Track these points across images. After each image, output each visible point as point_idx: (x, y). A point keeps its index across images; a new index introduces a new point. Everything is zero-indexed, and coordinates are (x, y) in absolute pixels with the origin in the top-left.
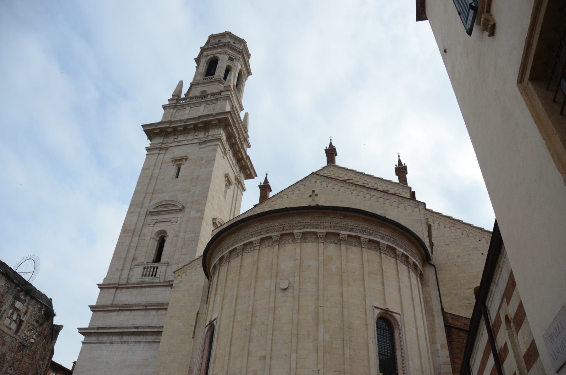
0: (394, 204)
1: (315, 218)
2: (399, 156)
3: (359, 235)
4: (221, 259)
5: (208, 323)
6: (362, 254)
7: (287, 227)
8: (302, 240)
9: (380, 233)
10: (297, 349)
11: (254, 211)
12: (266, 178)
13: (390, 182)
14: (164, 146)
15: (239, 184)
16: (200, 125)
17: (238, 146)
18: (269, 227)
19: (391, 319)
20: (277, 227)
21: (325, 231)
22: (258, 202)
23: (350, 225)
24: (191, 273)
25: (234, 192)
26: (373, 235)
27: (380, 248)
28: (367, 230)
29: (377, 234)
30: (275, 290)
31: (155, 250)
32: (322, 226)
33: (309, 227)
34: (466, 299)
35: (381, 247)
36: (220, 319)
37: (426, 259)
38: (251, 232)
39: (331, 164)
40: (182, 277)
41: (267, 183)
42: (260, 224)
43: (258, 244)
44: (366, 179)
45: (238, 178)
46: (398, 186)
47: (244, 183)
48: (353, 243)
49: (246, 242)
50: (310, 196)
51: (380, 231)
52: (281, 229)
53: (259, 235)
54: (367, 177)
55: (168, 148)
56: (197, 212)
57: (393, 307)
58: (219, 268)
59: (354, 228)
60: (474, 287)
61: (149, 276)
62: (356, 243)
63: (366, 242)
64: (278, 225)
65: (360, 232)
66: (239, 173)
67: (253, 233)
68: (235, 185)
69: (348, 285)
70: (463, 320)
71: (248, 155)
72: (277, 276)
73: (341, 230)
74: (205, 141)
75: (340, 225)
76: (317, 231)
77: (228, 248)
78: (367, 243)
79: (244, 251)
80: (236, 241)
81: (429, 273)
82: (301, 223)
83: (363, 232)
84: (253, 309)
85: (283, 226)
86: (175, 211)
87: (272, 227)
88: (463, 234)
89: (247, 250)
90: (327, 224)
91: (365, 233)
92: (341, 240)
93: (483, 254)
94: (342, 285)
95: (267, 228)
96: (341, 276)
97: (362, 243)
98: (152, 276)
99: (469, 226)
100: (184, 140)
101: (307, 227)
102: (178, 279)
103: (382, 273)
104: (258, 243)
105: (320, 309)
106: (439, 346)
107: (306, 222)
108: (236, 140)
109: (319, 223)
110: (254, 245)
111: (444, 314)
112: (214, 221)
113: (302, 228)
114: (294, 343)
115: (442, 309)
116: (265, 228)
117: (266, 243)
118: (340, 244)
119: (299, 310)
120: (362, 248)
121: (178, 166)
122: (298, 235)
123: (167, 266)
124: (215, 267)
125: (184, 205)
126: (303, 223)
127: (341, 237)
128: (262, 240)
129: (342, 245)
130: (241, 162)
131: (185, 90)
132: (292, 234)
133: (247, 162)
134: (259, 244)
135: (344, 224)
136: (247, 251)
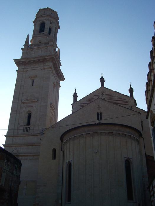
3: (119, 132)
5: (67, 161)
14: (25, 70)
16: (41, 60)
21: (108, 132)
37: (140, 135)
49: (81, 134)
50: (98, 108)
61: (26, 131)
74: (44, 68)
81: (141, 140)
98: (28, 131)
100: (34, 67)
115: (145, 154)
131: (31, 39)
132: (97, 133)
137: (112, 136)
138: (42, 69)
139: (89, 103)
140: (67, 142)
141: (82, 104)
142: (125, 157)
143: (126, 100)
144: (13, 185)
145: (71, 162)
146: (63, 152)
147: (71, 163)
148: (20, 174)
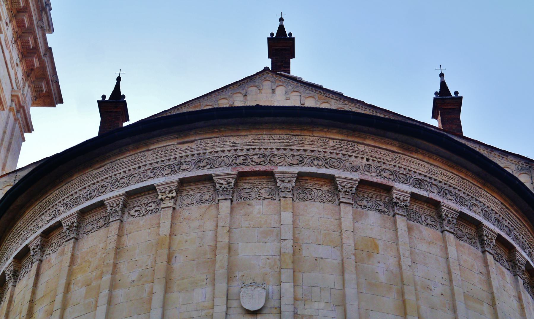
2: (442, 75)
3: (436, 197)
4: (47, 234)
6: (446, 247)
7: (256, 157)
8: (295, 195)
9: (480, 202)
12: (117, 87)
15: (18, 111)
17: (30, 17)
18: (204, 153)
20: (227, 153)
21: (356, 176)
23: (415, 172)
25: (6, 127)
26: (467, 205)
27: (483, 240)
28: (453, 191)
29: (475, 205)
30: (226, 314)
32: (347, 165)
38: (149, 162)
39: (282, 73)
41: (120, 99)
42: (178, 144)
43: (170, 195)
47: (31, 111)
48: (423, 218)
51: (482, 200)
53: (174, 172)
58: (38, 257)
59: (426, 181)
62: (429, 217)
63: (452, 218)
64: (229, 151)
65: (439, 192)
66: (21, 85)
67: (156, 165)
68: (9, 112)
72: (229, 279)
73: (394, 180)
75: (393, 169)
76: (336, 175)
77: (76, 202)
78: (455, 221)
79: (126, 210)
80: (102, 186)
82: (292, 150)
83: (445, 193)
85: (245, 152)
87: (214, 155)
90: (361, 160)
91: (448, 196)
92: (396, 203)
95: (199, 154)
96: (402, 294)
97: (444, 220)
101: (309, 160)
103: (493, 299)
104: (170, 192)
109: (340, 156)
110: (160, 197)
113: (296, 162)
116: (193, 155)
118: (392, 214)
120: (442, 232)
124: (25, 253)
126: (298, 150)
127: (395, 196)
128: (183, 182)
129: (397, 216)
130: (30, 59)
133: (44, 61)
134: (174, 195)
135: (400, 167)
136: (136, 211)
137: (380, 211)
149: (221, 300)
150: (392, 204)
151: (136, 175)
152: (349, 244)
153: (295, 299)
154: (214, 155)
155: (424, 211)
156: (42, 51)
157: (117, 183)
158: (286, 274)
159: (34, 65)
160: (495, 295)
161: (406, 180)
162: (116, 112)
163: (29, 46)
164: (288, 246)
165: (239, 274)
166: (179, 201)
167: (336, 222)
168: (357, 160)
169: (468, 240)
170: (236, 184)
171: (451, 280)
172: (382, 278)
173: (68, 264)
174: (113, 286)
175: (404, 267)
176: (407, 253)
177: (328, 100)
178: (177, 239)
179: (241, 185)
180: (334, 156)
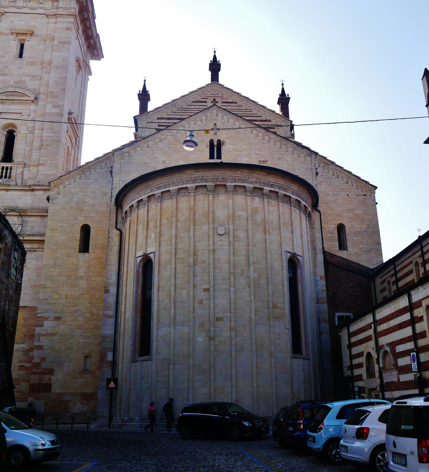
0: (290, 150)
1: (245, 173)
5: (140, 253)
6: (279, 207)
7: (220, 179)
10: (234, 284)
11: (156, 137)
13: (273, 112)
19: (296, 261)
21: (252, 186)
22: (138, 113)
24: (69, 184)
28: (283, 187)
31: (3, 147)
33: (240, 181)
34: (330, 233)
35: (292, 201)
36: (159, 253)
37: (315, 205)
39: (216, 82)
40: (59, 188)
43: (193, 191)
44: (251, 105)
45: (86, 61)
46: (280, 117)
51: (292, 187)
52: (215, 180)
54: (252, 103)
55: (3, 13)
56: (54, 107)
57: (298, 252)
58: (147, 204)
60: (338, 224)
62: (274, 197)
69: (270, 234)
70: (337, 258)
71: (98, 33)
72: (214, 223)
74: (55, 15)
75: (264, 182)
81: (315, 216)
83: (280, 188)
84: (194, 249)
85: (217, 177)
86: (26, 102)
88: (333, 175)
89: (182, 194)
91: (281, 189)
92: (264, 194)
93: (348, 195)
94: (265, 233)
96: (265, 226)
99: (340, 168)
100: (25, 7)
102: (55, 191)
103: (292, 223)
105: (251, 253)
106: (318, 278)
107: (236, 176)
108: (88, 15)
109: (247, 178)
110: (189, 191)
111: (324, 252)
112: (70, 117)
114: (232, 280)
115: (323, 248)
116: (200, 177)
117: (201, 191)
118: (263, 198)
119: (234, 253)
121: (20, 42)
122: (230, 188)
123: (23, 167)
125: (37, 96)
127: (264, 192)
129: (265, 199)
132: (225, 186)
134: (194, 191)
136: (181, 195)
138: (47, 16)
139: (183, 119)
140: (138, 207)
141: (162, 118)
142: (289, 251)
143: (270, 121)
144: (7, 308)
145: (152, 256)
146: (118, 232)
147: (153, 259)
148: (21, 281)
149: (211, 230)
150: (263, 194)
151: (180, 182)
152: (250, 210)
153: (234, 230)
154: (206, 178)
155: (273, 195)
156: (95, 36)
157: (174, 184)
158: (231, 222)
159: (91, 43)
160: (293, 222)
161: (268, 185)
162: (146, 99)
163: (89, 35)
164: (231, 212)
165: (216, 221)
166: (195, 193)
167: (246, 202)
168: (253, 179)
169: (286, 202)
170: (214, 188)
171: (280, 219)
172: (259, 221)
173: (160, 211)
174: (177, 222)
175: (266, 217)
176: (267, 212)
177: (239, 120)
178: (196, 207)
179: (216, 189)
180: (245, 178)
